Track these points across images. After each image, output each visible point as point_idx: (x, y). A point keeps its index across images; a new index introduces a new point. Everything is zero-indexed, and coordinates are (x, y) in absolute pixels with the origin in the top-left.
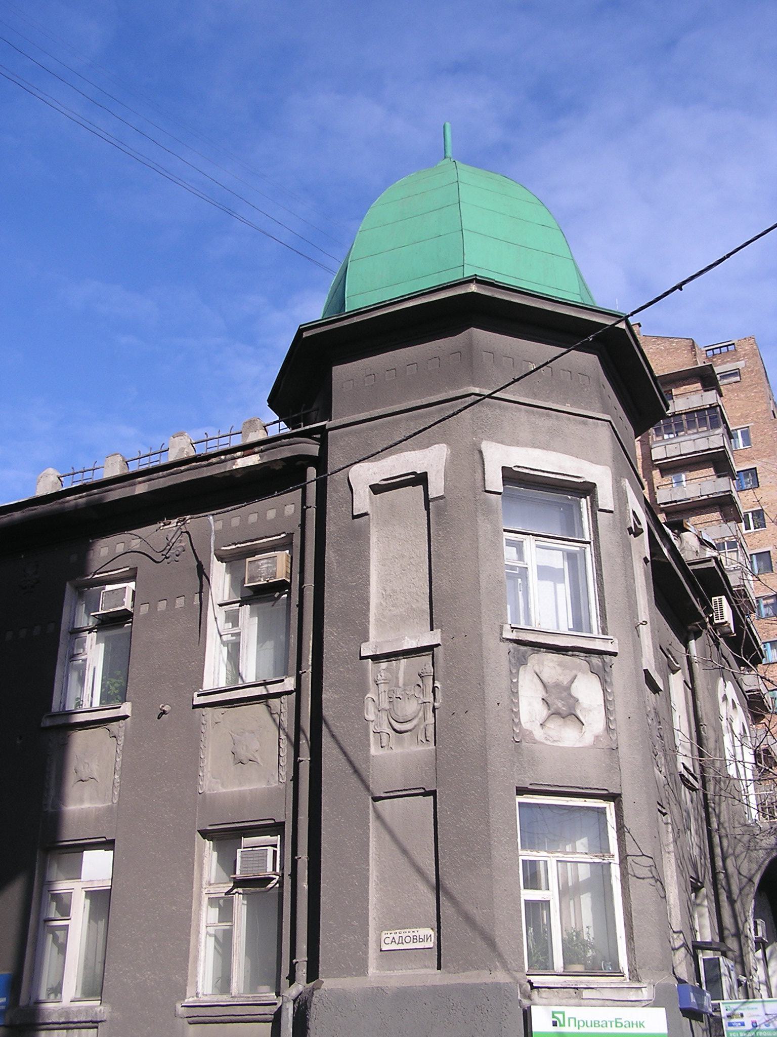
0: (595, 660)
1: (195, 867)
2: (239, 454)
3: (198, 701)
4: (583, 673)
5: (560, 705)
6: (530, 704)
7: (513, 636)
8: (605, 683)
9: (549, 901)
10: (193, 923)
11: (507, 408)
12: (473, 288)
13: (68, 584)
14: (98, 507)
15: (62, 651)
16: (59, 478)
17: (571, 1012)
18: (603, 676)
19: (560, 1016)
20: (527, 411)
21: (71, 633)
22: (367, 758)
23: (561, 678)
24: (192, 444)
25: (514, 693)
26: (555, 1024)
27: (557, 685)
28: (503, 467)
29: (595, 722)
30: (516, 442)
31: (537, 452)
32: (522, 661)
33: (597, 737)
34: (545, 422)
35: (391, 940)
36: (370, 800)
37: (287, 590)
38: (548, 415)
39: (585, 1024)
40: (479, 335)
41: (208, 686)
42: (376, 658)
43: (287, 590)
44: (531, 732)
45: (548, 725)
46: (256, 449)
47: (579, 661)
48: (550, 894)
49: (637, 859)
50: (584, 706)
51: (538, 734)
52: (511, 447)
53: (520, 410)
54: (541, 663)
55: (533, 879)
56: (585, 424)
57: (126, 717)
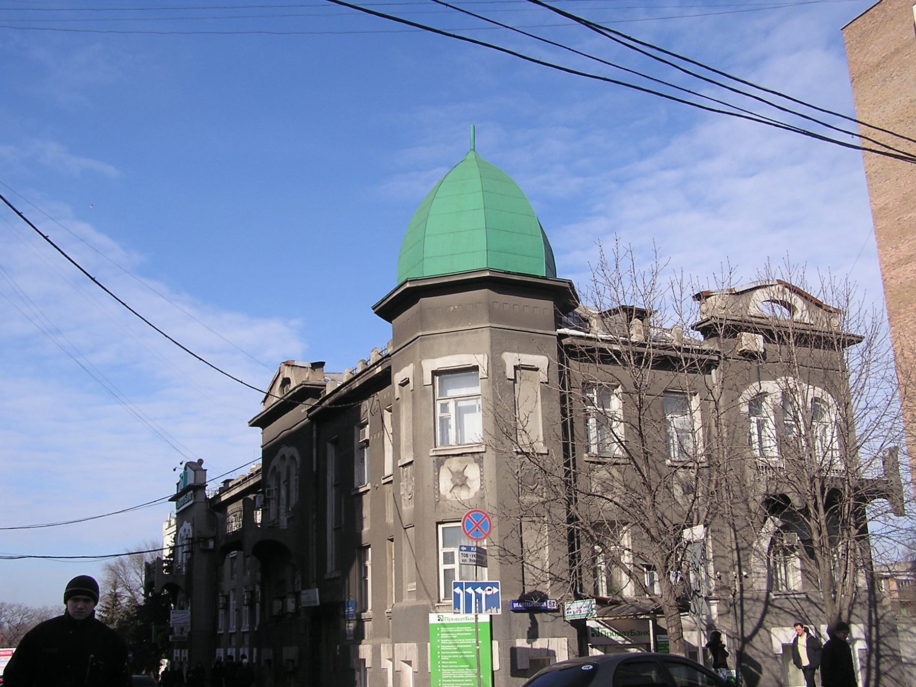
0: (477, 456)
1: (388, 554)
2: (376, 366)
3: (383, 482)
4: (472, 463)
5: (458, 481)
6: (445, 483)
7: (434, 454)
8: (480, 467)
9: (445, 570)
10: (389, 579)
11: (436, 338)
12: (408, 285)
13: (355, 427)
14: (351, 392)
15: (357, 458)
16: (351, 373)
17: (445, 615)
18: (479, 462)
19: (441, 617)
20: (446, 336)
21: (360, 449)
22: (402, 511)
23: (460, 468)
24: (379, 354)
25: (437, 479)
26: (439, 620)
27: (458, 472)
28: (432, 371)
29: (475, 486)
30: (441, 356)
31: (449, 357)
32: (442, 463)
33: (476, 493)
34: (454, 339)
35: (410, 585)
36: (403, 529)
37: (261, 490)
38: (457, 334)
39: (452, 619)
40: (423, 301)
41: (386, 475)
42: (403, 466)
43: (261, 490)
44: (445, 496)
45: (453, 491)
46: (379, 364)
47: (470, 458)
48: (456, 566)
49: (491, 547)
50: (471, 479)
51: (449, 496)
52: (436, 360)
53: (442, 336)
54: (450, 462)
55: (449, 558)
56: (476, 332)
57: (369, 490)
